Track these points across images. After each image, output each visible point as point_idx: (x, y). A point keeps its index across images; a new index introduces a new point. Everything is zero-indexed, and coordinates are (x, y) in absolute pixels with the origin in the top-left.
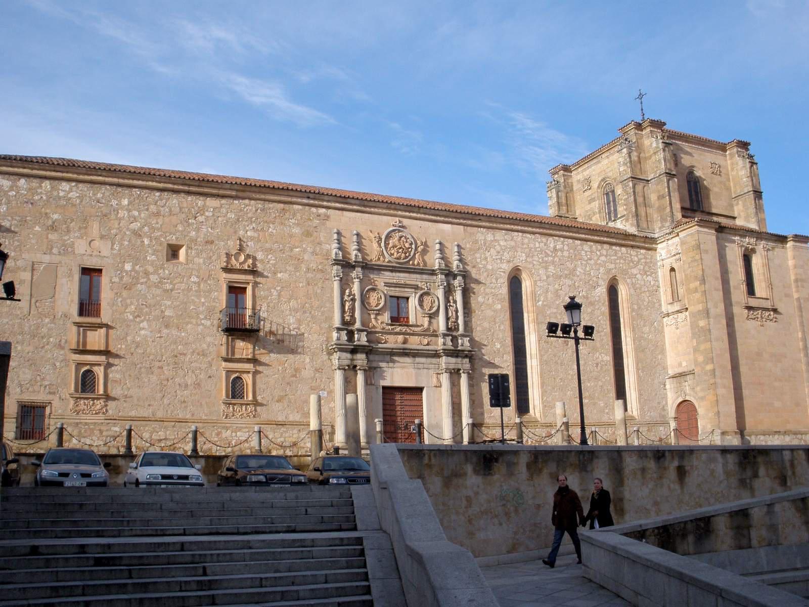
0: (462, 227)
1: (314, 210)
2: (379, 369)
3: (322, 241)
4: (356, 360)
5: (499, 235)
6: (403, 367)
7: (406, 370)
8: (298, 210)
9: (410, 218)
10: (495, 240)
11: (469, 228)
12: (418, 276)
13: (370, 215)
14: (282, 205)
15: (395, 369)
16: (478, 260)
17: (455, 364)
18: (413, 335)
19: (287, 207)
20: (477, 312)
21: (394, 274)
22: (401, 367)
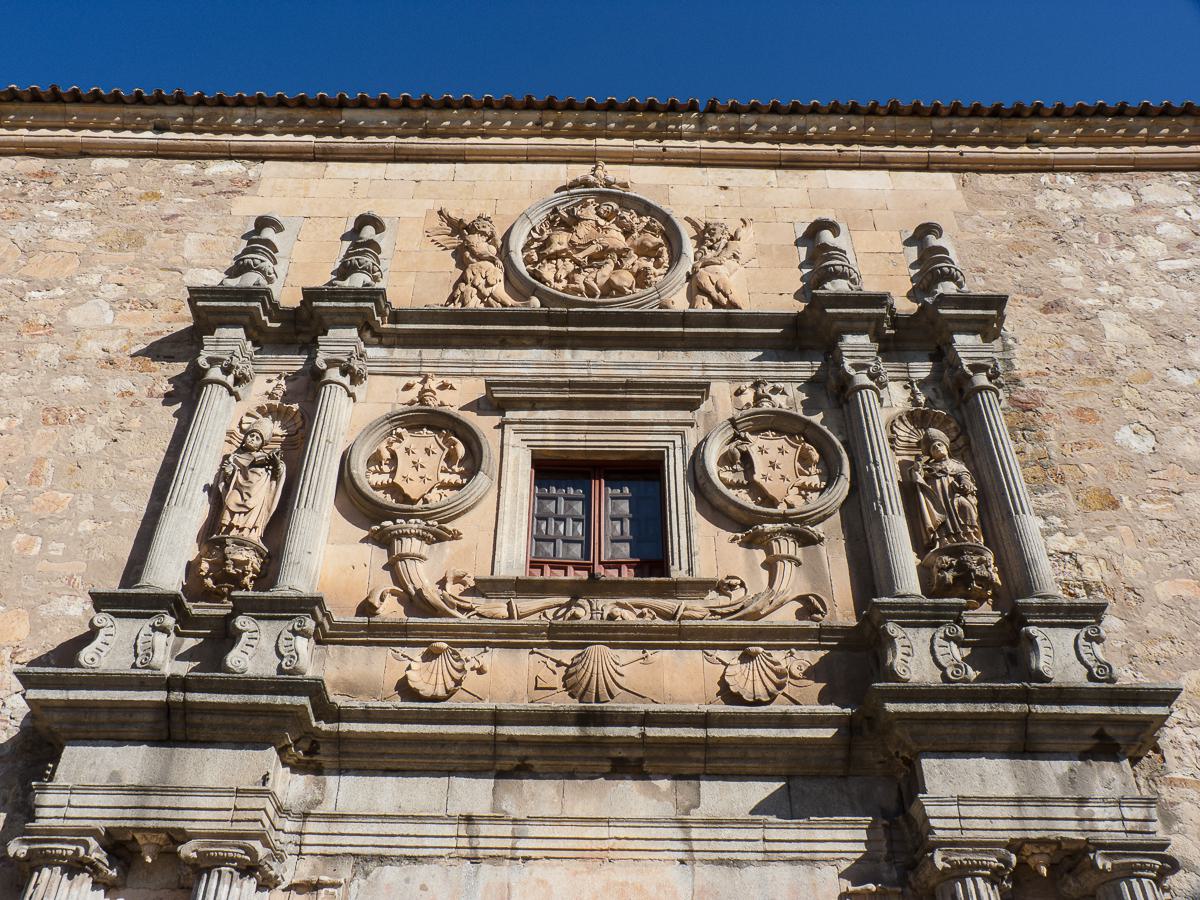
0: (948, 179)
1: (186, 168)
2: (390, 873)
3: (188, 264)
4: (179, 791)
5: (1158, 189)
6: (603, 856)
7: (619, 874)
8: (106, 174)
9: (662, 160)
10: (1146, 206)
11: (985, 179)
12: (713, 357)
13: (459, 166)
14: (38, 164)
15: (538, 870)
16: (1066, 282)
17: (1019, 801)
18: (679, 636)
19: (63, 166)
20: (1127, 503)
21: (567, 355)
22: (580, 855)
